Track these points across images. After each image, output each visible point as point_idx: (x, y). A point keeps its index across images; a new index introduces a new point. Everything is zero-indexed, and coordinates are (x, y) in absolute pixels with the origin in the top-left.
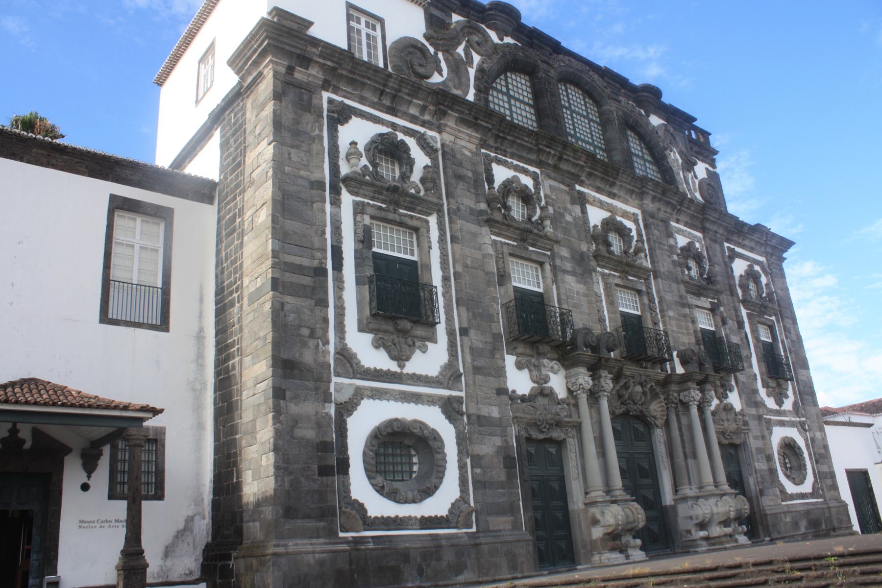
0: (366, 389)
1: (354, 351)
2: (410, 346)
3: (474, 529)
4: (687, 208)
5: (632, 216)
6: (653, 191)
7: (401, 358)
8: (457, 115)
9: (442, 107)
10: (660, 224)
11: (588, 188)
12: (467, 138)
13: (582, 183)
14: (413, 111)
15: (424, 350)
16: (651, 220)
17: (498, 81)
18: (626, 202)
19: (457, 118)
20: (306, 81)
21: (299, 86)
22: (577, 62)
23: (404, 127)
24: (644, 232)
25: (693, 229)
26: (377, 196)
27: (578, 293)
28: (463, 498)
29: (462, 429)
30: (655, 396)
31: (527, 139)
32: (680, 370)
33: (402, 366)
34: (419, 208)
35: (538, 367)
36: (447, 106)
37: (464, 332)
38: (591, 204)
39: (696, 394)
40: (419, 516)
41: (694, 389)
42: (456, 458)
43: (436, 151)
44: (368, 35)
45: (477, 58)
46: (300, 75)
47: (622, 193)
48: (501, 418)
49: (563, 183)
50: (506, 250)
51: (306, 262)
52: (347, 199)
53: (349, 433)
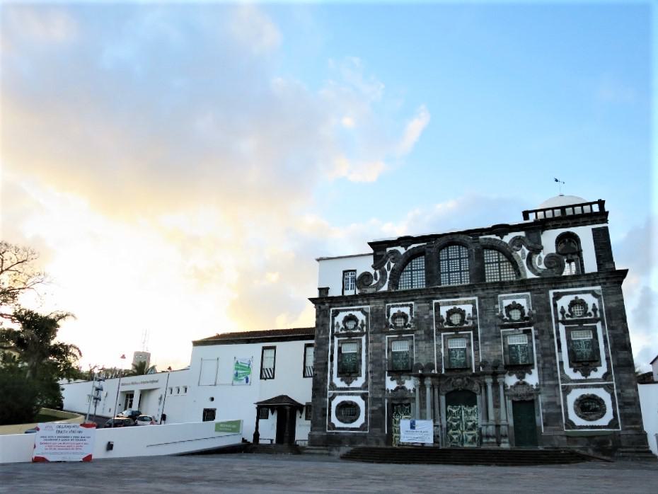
7: (348, 383)
10: (490, 299)
13: (437, 299)
14: (360, 302)
15: (357, 380)
16: (482, 300)
18: (468, 296)
24: (477, 308)
35: (401, 379)
47: (464, 294)
49: (426, 302)
50: (390, 340)
52: (336, 339)
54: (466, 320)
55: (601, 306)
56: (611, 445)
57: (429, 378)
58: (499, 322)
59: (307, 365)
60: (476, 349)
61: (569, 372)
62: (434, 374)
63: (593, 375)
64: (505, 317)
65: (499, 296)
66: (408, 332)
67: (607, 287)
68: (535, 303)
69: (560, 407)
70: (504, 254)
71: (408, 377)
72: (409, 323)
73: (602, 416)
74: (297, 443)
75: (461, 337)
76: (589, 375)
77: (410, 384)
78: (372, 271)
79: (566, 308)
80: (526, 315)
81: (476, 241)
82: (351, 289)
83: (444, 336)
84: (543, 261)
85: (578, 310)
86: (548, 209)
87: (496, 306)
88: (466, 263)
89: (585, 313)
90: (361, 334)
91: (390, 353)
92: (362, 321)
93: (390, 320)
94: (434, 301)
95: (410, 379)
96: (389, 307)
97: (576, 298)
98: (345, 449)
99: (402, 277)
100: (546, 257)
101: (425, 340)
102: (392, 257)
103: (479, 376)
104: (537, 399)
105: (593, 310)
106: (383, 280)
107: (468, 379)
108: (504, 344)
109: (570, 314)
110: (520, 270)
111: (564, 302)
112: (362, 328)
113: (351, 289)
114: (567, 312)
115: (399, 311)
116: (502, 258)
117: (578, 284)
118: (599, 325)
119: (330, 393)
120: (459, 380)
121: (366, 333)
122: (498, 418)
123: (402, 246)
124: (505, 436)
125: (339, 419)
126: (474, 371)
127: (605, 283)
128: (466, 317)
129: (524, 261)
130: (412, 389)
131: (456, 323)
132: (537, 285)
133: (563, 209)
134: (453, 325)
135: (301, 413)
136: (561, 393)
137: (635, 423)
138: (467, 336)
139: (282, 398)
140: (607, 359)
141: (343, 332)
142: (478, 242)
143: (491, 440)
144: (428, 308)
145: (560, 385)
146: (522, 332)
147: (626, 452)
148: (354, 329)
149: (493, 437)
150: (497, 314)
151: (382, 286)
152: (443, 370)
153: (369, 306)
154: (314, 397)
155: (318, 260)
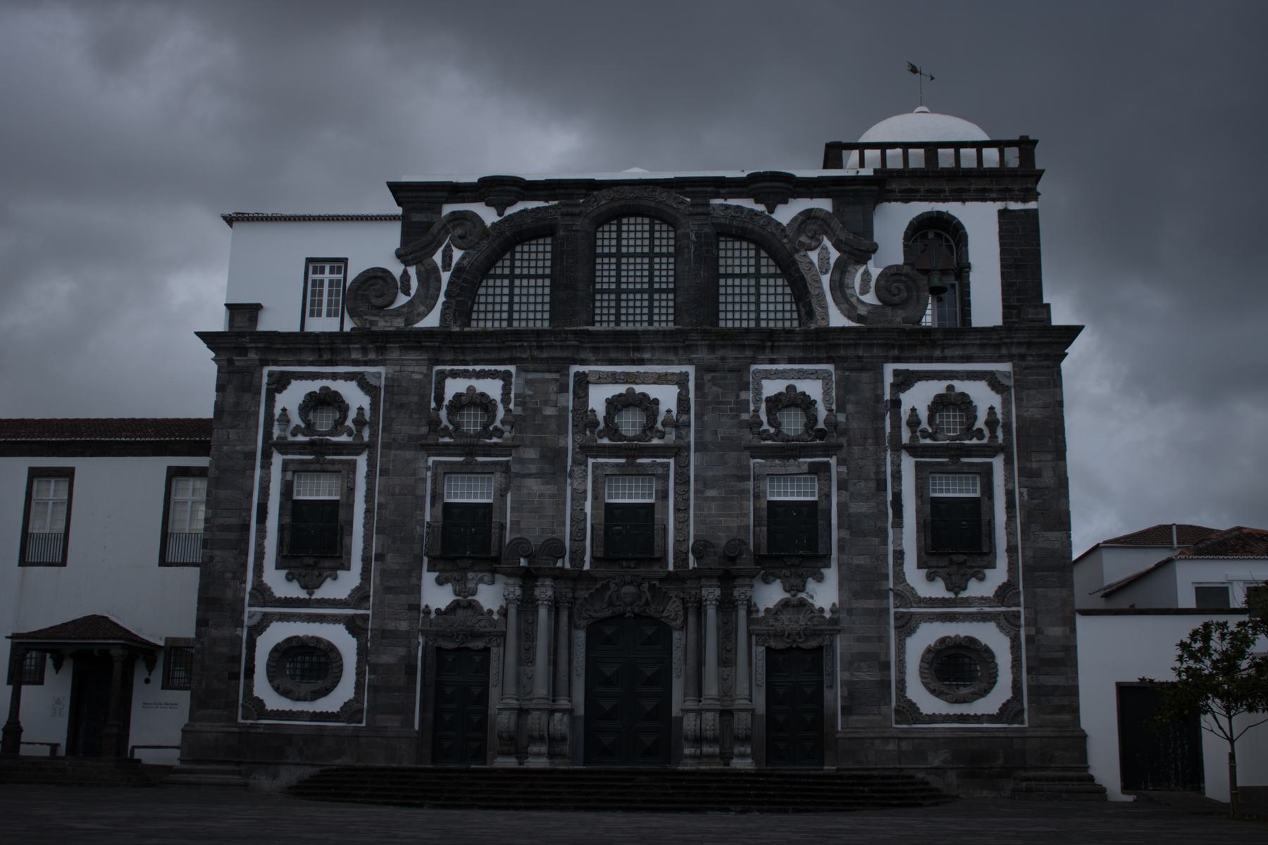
0: (275, 614)
1: (269, 585)
3: (364, 724)
4: (786, 341)
6: (702, 340)
7: (310, 587)
8: (397, 345)
9: (378, 344)
10: (729, 375)
11: (596, 364)
12: (414, 363)
13: (583, 362)
14: (355, 355)
16: (708, 377)
17: (500, 264)
22: (632, 187)
23: (346, 373)
26: (302, 451)
27: (540, 496)
29: (364, 641)
31: (490, 341)
33: (311, 594)
34: (345, 451)
36: (382, 342)
37: (380, 557)
40: (311, 711)
42: (354, 665)
43: (377, 388)
44: (331, 283)
47: (657, 355)
48: (408, 632)
49: (549, 371)
50: (440, 470)
51: (234, 521)
52: (277, 460)
53: (257, 648)
54: (659, 426)
55: (1007, 413)
56: (1000, 762)
57: (548, 582)
58: (748, 437)
59: (177, 526)
60: (682, 509)
61: (914, 576)
62: (562, 569)
63: (975, 589)
64: (766, 426)
65: (754, 367)
66: (489, 449)
67: (1026, 368)
68: (844, 394)
69: (886, 666)
70: (772, 255)
71: (487, 577)
72: (498, 423)
73: (985, 692)
74: (138, 754)
75: (642, 473)
76: (965, 589)
77: (489, 596)
78: (396, 269)
79: (923, 414)
80: (821, 425)
81: (700, 210)
82: (329, 315)
83: (595, 466)
84: (873, 284)
85: (951, 423)
86: (893, 145)
87: (743, 395)
88: (665, 270)
89: (969, 431)
90: (356, 449)
91: (439, 508)
92: (361, 409)
93: (443, 414)
94: (575, 369)
95: (492, 583)
96: (442, 376)
97: (950, 388)
98: (289, 775)
99: (482, 291)
100: (881, 275)
101: (540, 475)
102: (459, 231)
103: (683, 580)
104: (832, 646)
105: (987, 423)
106: (426, 299)
107: (652, 587)
108: (757, 497)
109: (930, 430)
110: (814, 301)
111: (919, 398)
112: (360, 431)
113: (329, 315)
114: (924, 425)
115: (471, 389)
116: (768, 266)
117: (958, 352)
118: (998, 463)
119: (251, 613)
120: (629, 589)
121: (370, 447)
122: (726, 692)
123: (488, 204)
124: (747, 739)
125: (277, 689)
126: (671, 568)
127: (1022, 357)
128: (660, 419)
129: (826, 280)
130: (495, 608)
131: (631, 434)
132: (856, 346)
133: (931, 148)
134: (625, 438)
135: (151, 667)
136: (892, 632)
137: (1060, 709)
138: (660, 471)
139: (96, 624)
140: (1011, 550)
141: (300, 438)
142: (708, 214)
143: (707, 749)
144: (553, 387)
145: (892, 611)
146: (805, 468)
147: (1035, 779)
148: (336, 431)
149: (714, 741)
150: (745, 416)
151: (423, 315)
152: (587, 558)
153: (380, 369)
154: (201, 623)
155: (230, 220)
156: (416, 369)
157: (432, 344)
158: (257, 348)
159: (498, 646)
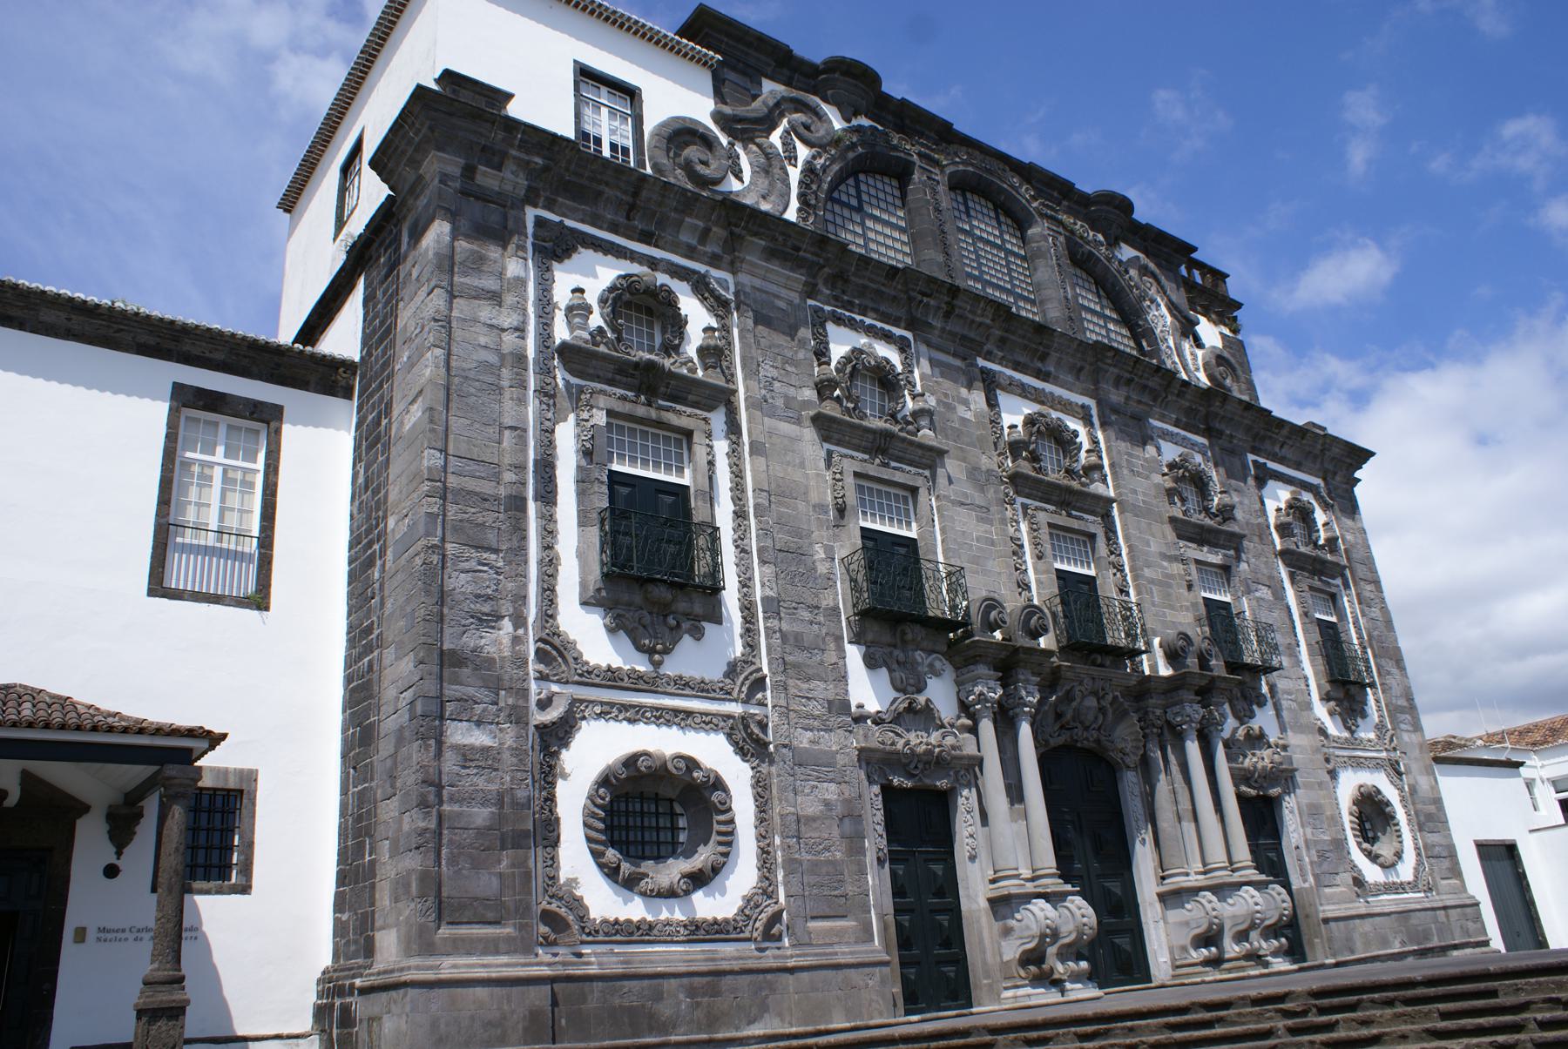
2: (672, 629)
4: (1178, 395)
5: (1080, 410)
8: (763, 243)
13: (988, 356)
17: (842, 187)
19: (765, 249)
20: (497, 189)
21: (483, 197)
25: (1190, 432)
26: (618, 377)
28: (766, 889)
30: (1122, 715)
32: (1165, 671)
33: (657, 665)
36: (743, 229)
37: (773, 607)
38: (1003, 389)
39: (1195, 711)
41: (1191, 702)
45: (803, 152)
46: (487, 178)
49: (955, 355)
96: (819, 322)
156: (784, 292)
157: (815, 258)
158: (525, 165)
159: (969, 786)
